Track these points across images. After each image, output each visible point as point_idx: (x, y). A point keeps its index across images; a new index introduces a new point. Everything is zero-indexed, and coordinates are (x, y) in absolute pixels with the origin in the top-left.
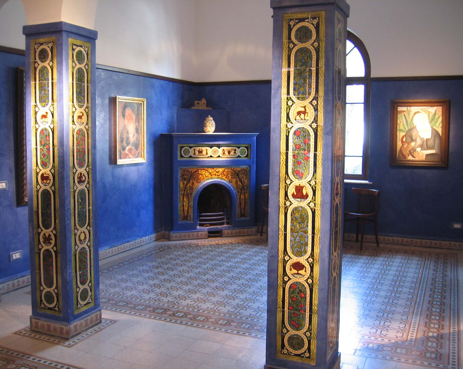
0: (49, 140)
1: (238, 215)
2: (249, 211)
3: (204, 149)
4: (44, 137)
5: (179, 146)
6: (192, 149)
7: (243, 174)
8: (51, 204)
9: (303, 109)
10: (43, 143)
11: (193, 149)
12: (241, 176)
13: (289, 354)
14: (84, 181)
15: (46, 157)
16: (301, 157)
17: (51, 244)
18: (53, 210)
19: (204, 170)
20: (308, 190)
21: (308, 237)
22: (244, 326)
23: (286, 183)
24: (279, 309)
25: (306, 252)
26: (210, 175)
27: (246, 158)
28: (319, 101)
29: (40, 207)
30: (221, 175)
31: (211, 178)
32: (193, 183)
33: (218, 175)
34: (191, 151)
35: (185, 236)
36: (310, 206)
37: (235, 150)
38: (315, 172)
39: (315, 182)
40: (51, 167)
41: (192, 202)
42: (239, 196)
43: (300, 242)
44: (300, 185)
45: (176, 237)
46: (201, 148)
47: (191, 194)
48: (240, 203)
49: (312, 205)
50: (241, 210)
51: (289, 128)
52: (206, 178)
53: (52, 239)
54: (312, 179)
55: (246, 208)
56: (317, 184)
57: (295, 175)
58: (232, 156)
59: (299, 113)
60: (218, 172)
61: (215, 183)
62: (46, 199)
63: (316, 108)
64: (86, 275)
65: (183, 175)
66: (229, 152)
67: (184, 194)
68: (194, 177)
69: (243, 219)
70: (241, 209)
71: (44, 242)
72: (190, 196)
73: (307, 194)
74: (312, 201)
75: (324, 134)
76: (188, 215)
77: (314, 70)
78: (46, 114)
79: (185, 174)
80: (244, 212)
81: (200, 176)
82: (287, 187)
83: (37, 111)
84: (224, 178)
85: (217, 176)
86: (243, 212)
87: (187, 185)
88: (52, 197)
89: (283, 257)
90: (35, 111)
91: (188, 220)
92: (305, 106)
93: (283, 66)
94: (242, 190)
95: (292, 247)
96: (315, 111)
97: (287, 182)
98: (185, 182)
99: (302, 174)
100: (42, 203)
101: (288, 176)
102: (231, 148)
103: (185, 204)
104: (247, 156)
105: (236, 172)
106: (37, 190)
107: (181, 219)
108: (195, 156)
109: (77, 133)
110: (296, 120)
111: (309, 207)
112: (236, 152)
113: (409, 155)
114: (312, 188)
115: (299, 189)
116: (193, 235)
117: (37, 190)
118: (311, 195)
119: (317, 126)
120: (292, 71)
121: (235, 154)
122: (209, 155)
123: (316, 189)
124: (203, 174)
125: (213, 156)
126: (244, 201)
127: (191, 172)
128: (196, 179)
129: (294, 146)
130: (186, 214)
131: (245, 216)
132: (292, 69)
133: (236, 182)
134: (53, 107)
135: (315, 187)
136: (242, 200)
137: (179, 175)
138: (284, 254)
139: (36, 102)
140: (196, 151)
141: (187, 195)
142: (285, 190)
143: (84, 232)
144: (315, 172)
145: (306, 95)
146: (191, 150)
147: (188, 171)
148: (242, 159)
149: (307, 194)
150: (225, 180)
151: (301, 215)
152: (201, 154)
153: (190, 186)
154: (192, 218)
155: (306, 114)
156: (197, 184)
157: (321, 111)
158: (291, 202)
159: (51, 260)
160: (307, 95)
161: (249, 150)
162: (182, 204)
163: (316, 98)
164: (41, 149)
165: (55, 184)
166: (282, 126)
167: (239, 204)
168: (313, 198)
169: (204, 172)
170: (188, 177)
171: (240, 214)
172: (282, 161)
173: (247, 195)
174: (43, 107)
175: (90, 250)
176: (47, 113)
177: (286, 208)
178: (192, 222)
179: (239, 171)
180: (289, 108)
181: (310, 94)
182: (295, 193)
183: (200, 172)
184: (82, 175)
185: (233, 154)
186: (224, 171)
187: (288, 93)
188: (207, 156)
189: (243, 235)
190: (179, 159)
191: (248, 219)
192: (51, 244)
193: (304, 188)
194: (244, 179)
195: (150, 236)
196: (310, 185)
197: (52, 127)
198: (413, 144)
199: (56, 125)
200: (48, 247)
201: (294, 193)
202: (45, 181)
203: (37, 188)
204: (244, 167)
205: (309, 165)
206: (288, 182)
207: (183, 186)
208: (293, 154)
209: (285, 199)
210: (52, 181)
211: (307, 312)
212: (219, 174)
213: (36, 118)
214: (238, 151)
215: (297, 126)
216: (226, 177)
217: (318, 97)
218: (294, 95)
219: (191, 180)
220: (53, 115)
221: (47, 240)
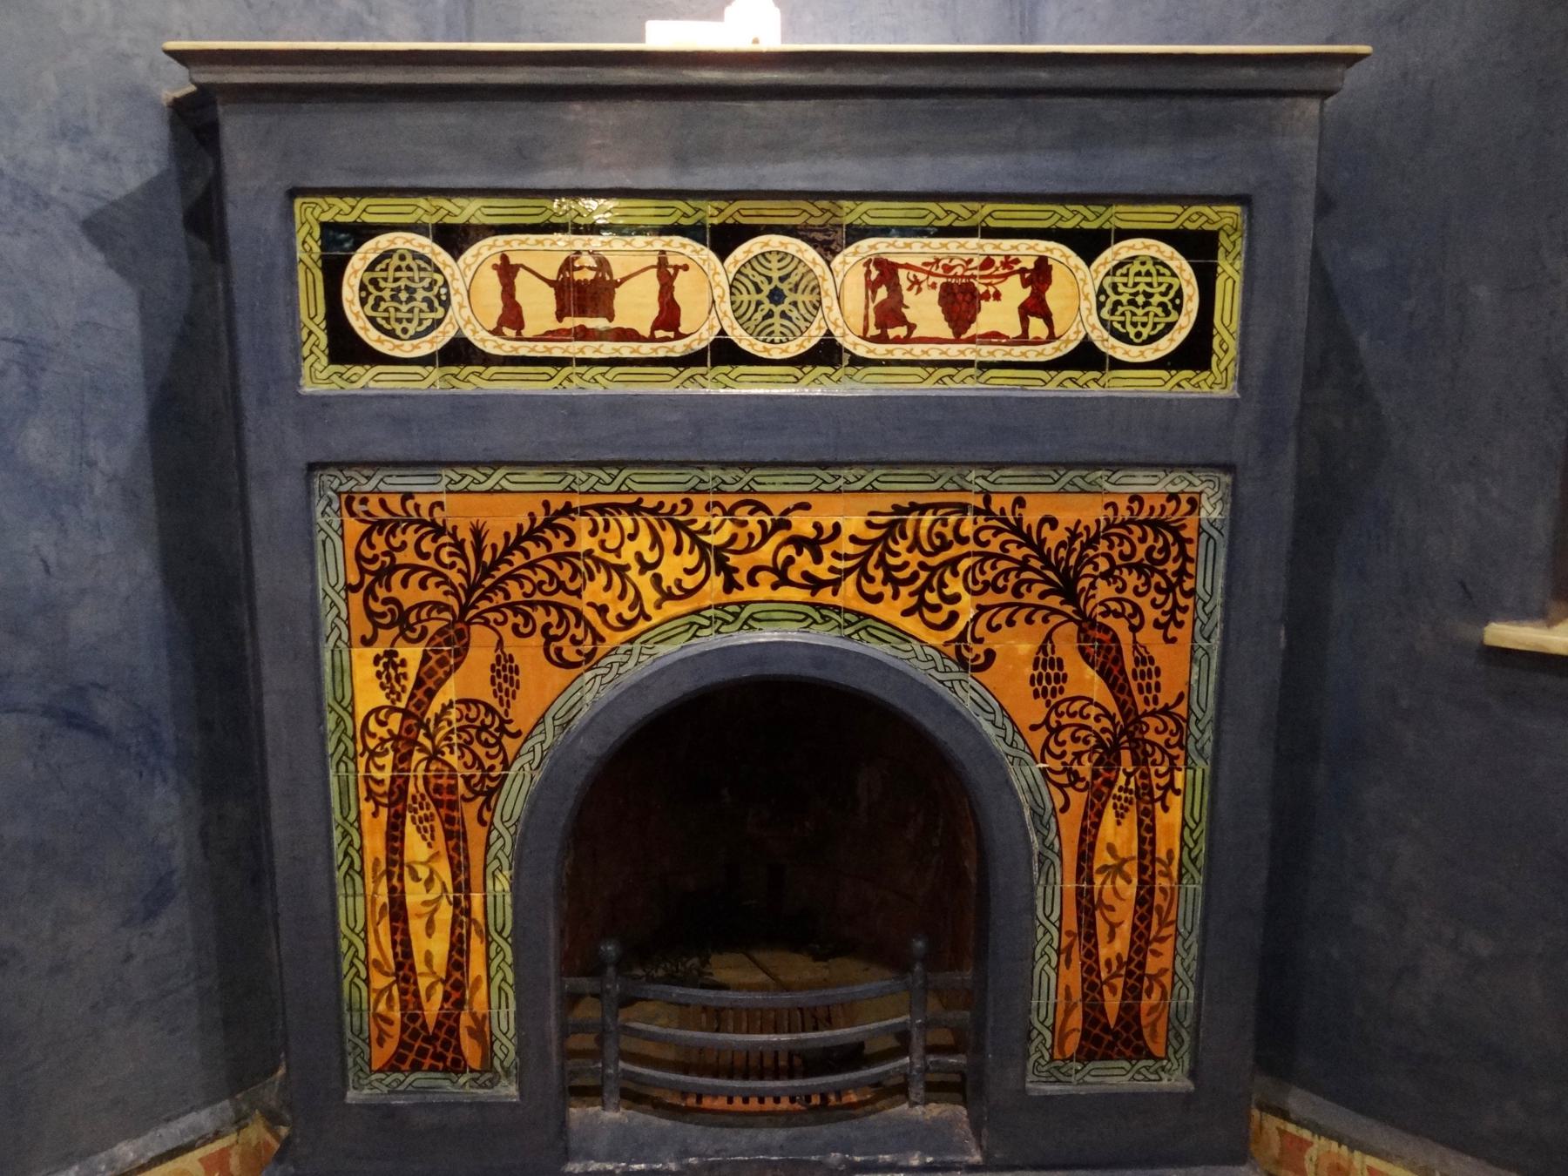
1: (1060, 1034)
2: (1187, 995)
5: (311, 215)
6: (469, 255)
7: (1132, 579)
11: (485, 251)
12: (1104, 590)
19: (634, 509)
26: (717, 582)
27: (1185, 384)
30: (849, 584)
32: (505, 671)
33: (814, 584)
34: (458, 285)
37: (1040, 275)
41: (503, 883)
42: (1070, 824)
46: (596, 242)
47: (488, 792)
48: (1088, 905)
50: (1092, 987)
52: (671, 608)
55: (1152, 965)
58: (1000, 353)
60: (812, 545)
61: (774, 670)
68: (516, 594)
69: (1117, 1077)
70: (1090, 969)
72: (470, 811)
76: (465, 1020)
79: (408, 557)
80: (1130, 1012)
81: (595, 591)
84: (889, 611)
85: (803, 595)
86: (1112, 1003)
87: (426, 686)
91: (458, 1066)
98: (411, 654)
102: (990, 246)
103: (415, 896)
105: (1039, 547)
107: (382, 1055)
108: (524, 349)
112: (1053, 298)
121: (1037, 327)
122: (698, 331)
124: (628, 556)
125: (746, 343)
126: (1130, 891)
127: (478, 534)
128: (539, 616)
130: (432, 1008)
131: (1142, 1052)
133: (1047, 663)
136: (1117, 870)
140: (522, 280)
141: (444, 799)
147: (439, 531)
148: (1119, 384)
150: (905, 636)
152: (599, 323)
153: (465, 702)
154: (506, 1049)
156: (560, 676)
161: (1229, 272)
162: (383, 897)
167: (1071, 923)
169: (644, 539)
170: (434, 593)
171: (1076, 1020)
173: (1169, 820)
178: (509, 1090)
179: (1085, 540)
183: (585, 543)
185: (1014, 330)
186: (893, 530)
188: (678, 348)
191: (1176, 1080)
194: (1149, 636)
207: (381, 699)
212: (822, 572)
219: (476, 630)
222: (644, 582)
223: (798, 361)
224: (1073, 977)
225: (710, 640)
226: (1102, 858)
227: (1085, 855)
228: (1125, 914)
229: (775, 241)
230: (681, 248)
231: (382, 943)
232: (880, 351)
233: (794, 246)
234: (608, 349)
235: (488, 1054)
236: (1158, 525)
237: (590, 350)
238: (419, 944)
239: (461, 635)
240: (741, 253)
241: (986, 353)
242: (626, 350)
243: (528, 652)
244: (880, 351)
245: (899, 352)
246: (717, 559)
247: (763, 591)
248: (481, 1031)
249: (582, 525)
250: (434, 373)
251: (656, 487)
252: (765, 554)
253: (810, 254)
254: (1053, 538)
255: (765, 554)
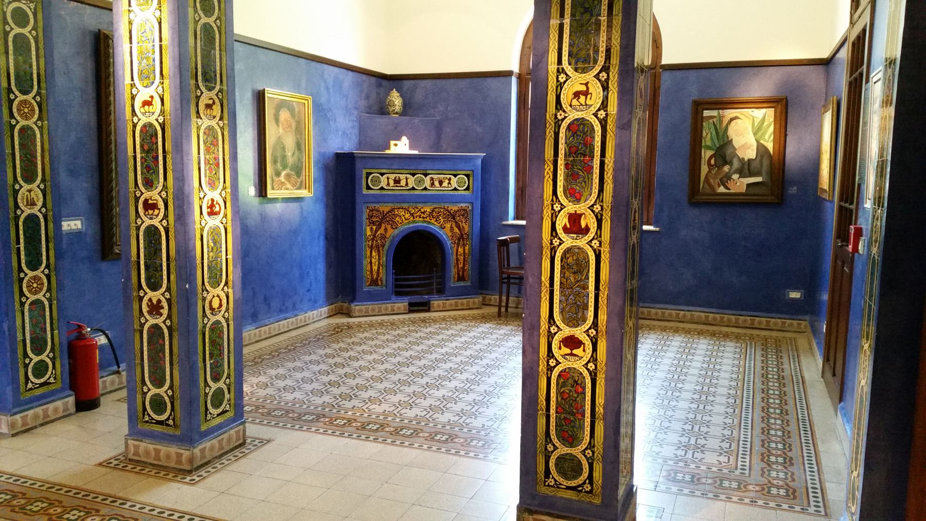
0: (157, 143)
2: (470, 272)
3: (402, 177)
4: (148, 138)
7: (461, 217)
8: (161, 250)
9: (584, 88)
10: (146, 148)
12: (458, 218)
13: (557, 486)
14: (218, 213)
15: (152, 171)
16: (579, 167)
17: (161, 315)
18: (164, 259)
19: (402, 208)
20: (589, 221)
21: (588, 294)
22: (475, 444)
23: (553, 209)
24: (541, 413)
25: (584, 320)
27: (467, 193)
28: (611, 73)
29: (142, 255)
31: (414, 222)
32: (386, 230)
33: (424, 218)
35: (373, 310)
36: (592, 245)
37: (450, 179)
38: (601, 190)
39: (602, 207)
40: (161, 188)
41: (385, 259)
43: (576, 303)
44: (576, 211)
45: (360, 311)
47: (383, 246)
48: (457, 260)
49: (595, 243)
51: (559, 120)
52: (407, 221)
53: (163, 308)
54: (595, 202)
55: (466, 268)
56: (604, 210)
57: (569, 196)
58: (445, 189)
59: (577, 95)
60: (423, 213)
62: (153, 242)
63: (605, 84)
64: (220, 365)
65: (370, 217)
66: (441, 183)
67: (372, 245)
69: (462, 284)
70: (458, 269)
71: (150, 313)
72: (381, 248)
73: (587, 226)
74: (596, 237)
75: (619, 127)
77: (604, 21)
78: (150, 100)
79: (374, 214)
80: (463, 274)
81: (397, 219)
82: (554, 215)
83: (134, 93)
84: (433, 221)
86: (461, 273)
87: (376, 231)
88: (164, 237)
89: (547, 327)
90: (132, 93)
91: (378, 285)
92: (588, 83)
93: (552, 15)
94: (459, 240)
95: (562, 311)
96: (604, 91)
97: (555, 208)
98: (374, 228)
99: (581, 195)
100: (145, 248)
101: (557, 198)
102: (444, 176)
103: (373, 261)
104: (467, 189)
106: (136, 227)
107: (368, 284)
108: (390, 188)
109: (204, 133)
110: (571, 106)
111: (591, 247)
112: (451, 182)
113: (719, 186)
114: (596, 217)
115: (575, 218)
116: (386, 309)
117: (136, 227)
118: (594, 228)
119: (607, 115)
120: (567, 23)
121: (450, 185)
122: (410, 186)
123: (603, 218)
124: (401, 214)
125: (416, 187)
126: (462, 258)
127: (383, 211)
129: (567, 149)
130: (375, 277)
131: (465, 280)
132: (567, 21)
133: (451, 227)
134: (163, 87)
135: (602, 215)
136: (461, 255)
137: (365, 216)
138: (549, 322)
139: (132, 80)
140: (390, 180)
141: (378, 247)
142: (552, 221)
143: (218, 296)
144: (601, 190)
145: (589, 64)
146: (384, 179)
147: (378, 211)
148: (459, 193)
149: (587, 226)
150: (435, 225)
151: (577, 260)
152: (398, 185)
154: (384, 282)
155: (589, 96)
156: (393, 230)
157: (614, 90)
158: (561, 240)
159: (161, 342)
160: (591, 64)
161: (471, 179)
163: (606, 69)
164: (142, 158)
165: (167, 217)
166: (547, 117)
168: (596, 233)
170: (378, 219)
171: (456, 276)
172: (548, 173)
173: (467, 248)
174: (146, 87)
175: (228, 325)
176: (152, 97)
177: (553, 250)
178: (384, 288)
180: (560, 86)
181: (595, 62)
182: (568, 226)
183: (396, 213)
184: (215, 203)
186: (433, 211)
187: (560, 62)
188: (408, 188)
189: (460, 308)
190: (365, 192)
191: (469, 284)
192: (161, 315)
193: (584, 215)
194: (464, 224)
195: (319, 310)
196: (593, 212)
197: (161, 121)
198: (726, 168)
199: (169, 117)
200: (157, 320)
201: (565, 225)
202: (151, 212)
203: (136, 223)
204: (464, 205)
205: (592, 179)
206: (557, 207)
208: (566, 162)
209: (552, 235)
210: (163, 210)
211: (587, 418)
212: (425, 216)
213: (133, 106)
214: (454, 180)
215: (573, 115)
216: (436, 221)
217: (609, 67)
218: (570, 64)
219: (383, 225)
220: (162, 100)
221: (155, 309)
222: (403, 218)
223: (422, 190)
224: (456, 270)
225: (411, 225)
226: (459, 253)
227: (457, 253)
228: (462, 261)
229: (419, 175)
230: (409, 176)
231: (369, 268)
232: (432, 188)
233: (422, 176)
234: (400, 188)
235: (382, 283)
236: (464, 210)
237: (397, 188)
238: (374, 267)
239: (381, 225)
240: (415, 176)
241: (444, 189)
242: (402, 188)
243: (389, 227)
244: (432, 188)
245: (434, 189)
246: (412, 215)
247: (418, 219)
248: (381, 280)
249: (396, 210)
250: (379, 191)
251: (405, 205)
252: (418, 214)
253: (424, 177)
254: (452, 212)
255: (418, 214)
